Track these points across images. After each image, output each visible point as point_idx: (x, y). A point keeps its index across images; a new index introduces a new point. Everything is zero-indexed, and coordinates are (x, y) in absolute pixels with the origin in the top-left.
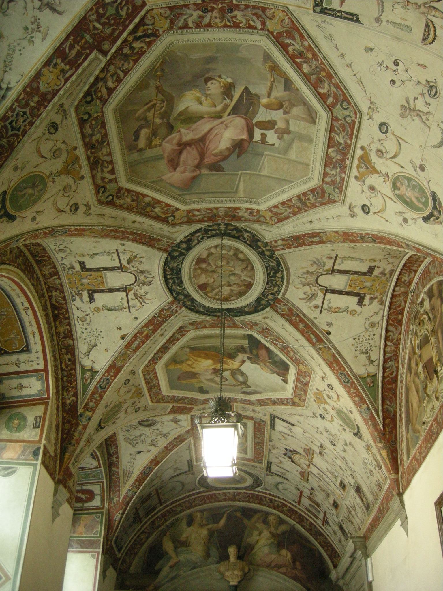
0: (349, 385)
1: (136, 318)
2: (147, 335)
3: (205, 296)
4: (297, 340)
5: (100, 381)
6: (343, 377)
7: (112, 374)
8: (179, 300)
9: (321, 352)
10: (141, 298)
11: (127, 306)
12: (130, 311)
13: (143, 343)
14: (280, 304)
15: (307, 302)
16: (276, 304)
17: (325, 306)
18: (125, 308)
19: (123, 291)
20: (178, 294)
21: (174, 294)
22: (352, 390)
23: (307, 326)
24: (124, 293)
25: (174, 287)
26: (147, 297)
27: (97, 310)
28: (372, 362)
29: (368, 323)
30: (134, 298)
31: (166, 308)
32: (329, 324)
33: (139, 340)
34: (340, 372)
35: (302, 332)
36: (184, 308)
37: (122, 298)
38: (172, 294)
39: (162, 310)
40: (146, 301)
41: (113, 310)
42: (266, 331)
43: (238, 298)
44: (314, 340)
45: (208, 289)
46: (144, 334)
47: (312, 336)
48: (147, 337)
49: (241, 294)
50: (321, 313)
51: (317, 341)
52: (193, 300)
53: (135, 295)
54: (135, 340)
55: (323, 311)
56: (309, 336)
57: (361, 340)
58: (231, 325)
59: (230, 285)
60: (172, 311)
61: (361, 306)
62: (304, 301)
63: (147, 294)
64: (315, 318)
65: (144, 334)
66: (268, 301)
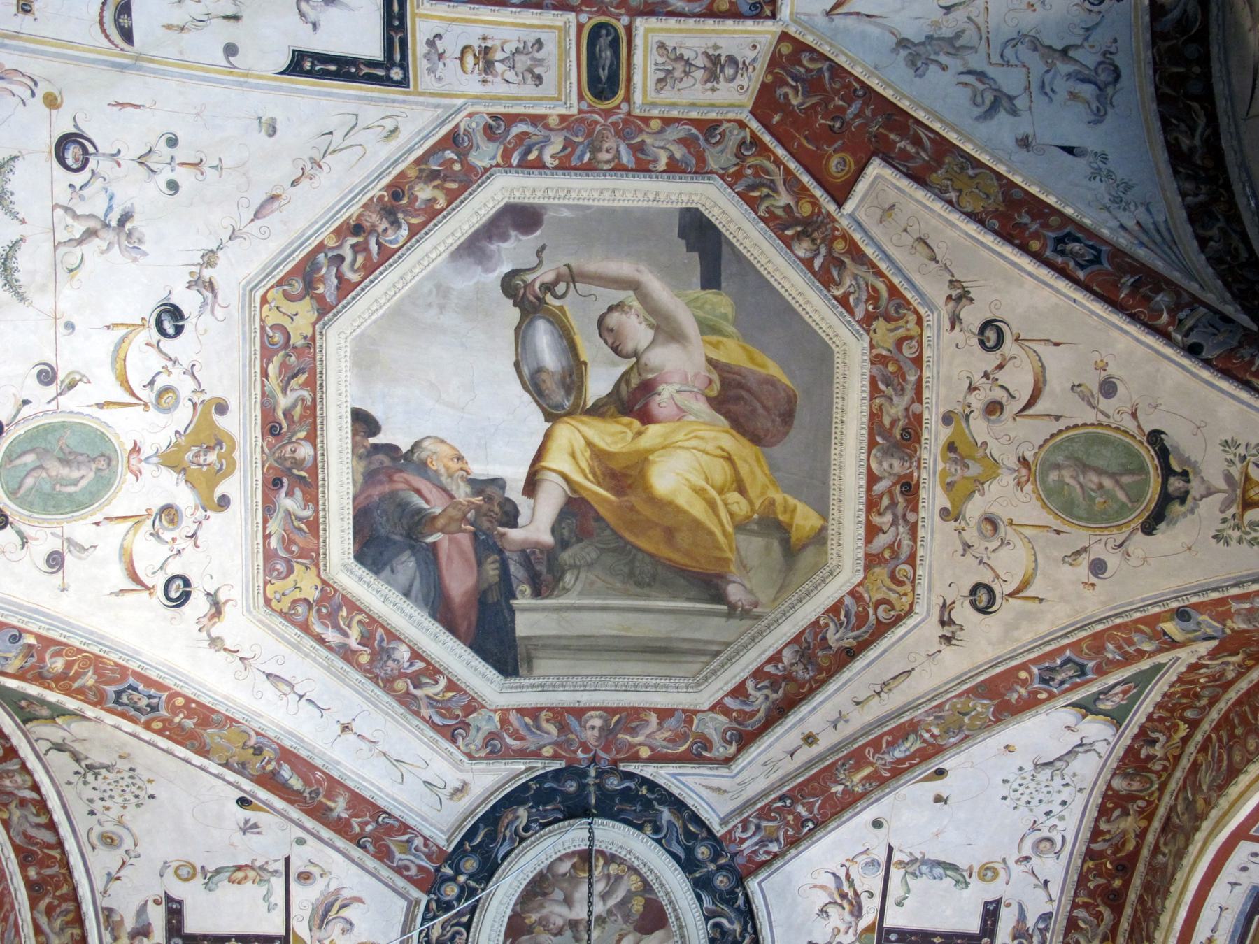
0: (110, 690)
1: (877, 824)
2: (857, 768)
3: (650, 878)
4: (345, 728)
5: (1075, 687)
6: (143, 702)
7: (1023, 691)
8: (729, 868)
9: (253, 740)
10: (844, 896)
11: (893, 870)
12: (891, 849)
13: (876, 744)
14: (421, 869)
15: (338, 891)
16: (430, 866)
17: (278, 883)
18: (900, 862)
19: (890, 931)
20: (728, 898)
21: (741, 901)
22: (89, 680)
23: (319, 813)
24: (888, 923)
25: (737, 928)
26: (822, 898)
27: (988, 872)
28: (60, 747)
29: (128, 843)
30: (864, 897)
31: (774, 848)
32: (249, 828)
33: (888, 758)
34: (164, 713)
35: (334, 786)
36: (719, 831)
37: (900, 904)
38: (747, 901)
39: (794, 842)
40: (831, 883)
41: (939, 864)
42: (453, 719)
43: (550, 867)
44: (286, 772)
45: (638, 905)
46: (867, 771)
47: (296, 783)
48: (857, 759)
49: (538, 888)
50: (287, 860)
51: (275, 774)
52: (688, 864)
53: (857, 911)
54: (900, 761)
55: (280, 866)
56: (307, 782)
57: (129, 796)
58: (572, 721)
59: (573, 924)
60: (758, 827)
61: (169, 899)
62: (346, 894)
63: (823, 912)
64: (300, 842)
65: (867, 771)
66: (458, 872)
